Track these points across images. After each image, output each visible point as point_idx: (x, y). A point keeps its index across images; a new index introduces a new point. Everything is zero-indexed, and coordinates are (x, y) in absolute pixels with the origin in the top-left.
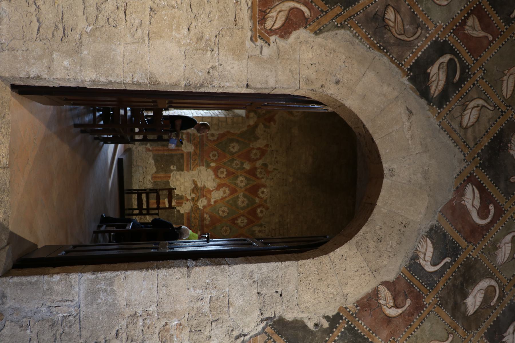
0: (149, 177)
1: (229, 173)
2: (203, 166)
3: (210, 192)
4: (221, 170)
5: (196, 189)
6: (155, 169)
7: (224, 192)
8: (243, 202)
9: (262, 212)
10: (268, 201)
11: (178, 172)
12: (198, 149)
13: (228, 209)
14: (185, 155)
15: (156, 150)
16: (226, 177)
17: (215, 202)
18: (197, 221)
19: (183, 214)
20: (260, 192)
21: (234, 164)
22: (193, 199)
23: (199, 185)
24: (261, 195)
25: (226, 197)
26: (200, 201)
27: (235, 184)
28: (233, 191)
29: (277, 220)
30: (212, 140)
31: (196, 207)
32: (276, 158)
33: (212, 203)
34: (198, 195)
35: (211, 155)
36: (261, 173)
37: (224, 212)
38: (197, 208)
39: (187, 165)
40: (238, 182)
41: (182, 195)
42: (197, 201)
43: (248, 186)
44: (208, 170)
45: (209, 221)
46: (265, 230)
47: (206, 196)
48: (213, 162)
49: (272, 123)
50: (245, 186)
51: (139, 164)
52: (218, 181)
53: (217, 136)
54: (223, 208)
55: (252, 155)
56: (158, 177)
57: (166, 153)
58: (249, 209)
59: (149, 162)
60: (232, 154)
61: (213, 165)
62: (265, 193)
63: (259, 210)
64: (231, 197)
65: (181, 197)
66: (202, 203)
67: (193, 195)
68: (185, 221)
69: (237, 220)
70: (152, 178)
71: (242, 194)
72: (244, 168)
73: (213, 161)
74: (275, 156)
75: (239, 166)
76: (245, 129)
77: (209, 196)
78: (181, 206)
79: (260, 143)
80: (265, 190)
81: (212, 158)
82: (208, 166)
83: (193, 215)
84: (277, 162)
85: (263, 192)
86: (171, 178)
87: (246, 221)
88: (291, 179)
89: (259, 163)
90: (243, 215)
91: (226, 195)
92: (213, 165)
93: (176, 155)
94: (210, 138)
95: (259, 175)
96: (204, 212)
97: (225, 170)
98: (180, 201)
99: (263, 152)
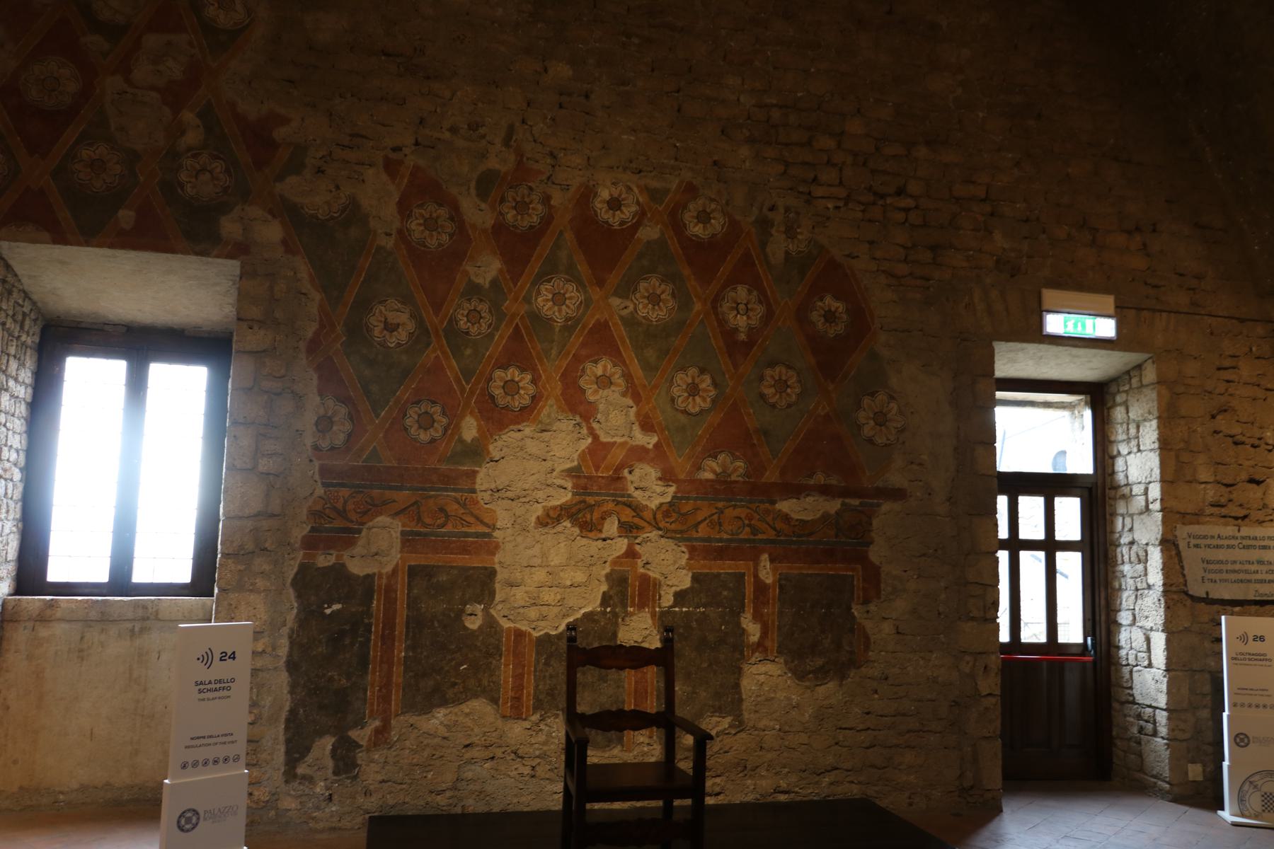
0: (517, 731)
1: (517, 355)
2: (475, 473)
3: (598, 450)
4: (498, 392)
5: (581, 516)
6: (479, 705)
7: (604, 382)
8: (654, 300)
9: (704, 217)
10: (655, 184)
11: (498, 598)
12: (389, 494)
13: (683, 369)
14: (415, 560)
15: (386, 699)
16: (534, 370)
17: (647, 426)
18: (730, 513)
19: (695, 578)
20: (614, 219)
21: (474, 330)
22: (627, 529)
23: (565, 497)
24: (628, 212)
25: (628, 376)
26: (637, 494)
27: (569, 328)
28: (601, 340)
29: (745, 151)
30: (348, 427)
31: (667, 514)
32: (454, 130)
33: (651, 441)
34: (611, 506)
35: (424, 437)
36: (522, 207)
37: (693, 390)
38: (669, 509)
39: (464, 550)
40: (558, 315)
41: (608, 576)
42: (637, 509)
43: (583, 268)
44: (496, 454)
45: (736, 458)
46: (787, 210)
47: (619, 469)
48: (458, 427)
49: (280, 133)
50: (581, 285)
51: (449, 777)
52: (549, 409)
53: (330, 403)
54: (675, 391)
55: (432, 243)
56: (519, 688)
57: (400, 652)
58: (686, 272)
59: (442, 731)
60: (422, 336)
61: (470, 429)
62: (617, 196)
63: (697, 230)
64: (629, 354)
65: (618, 581)
66: (649, 488)
67: (611, 527)
68: (726, 567)
69: (736, 330)
70: (519, 717)
71: (615, 302)
72: (494, 283)
73: (453, 427)
74: (447, 135)
75: (484, 308)
76: (303, 269)
77: (618, 456)
78: (657, 585)
79: (379, 198)
80: (605, 194)
81: (436, 432)
82: (476, 452)
83: (703, 531)
84: (474, 127)
85: (615, 204)
86: (524, 627)
87: (742, 292)
88: (561, 70)
89: (478, 214)
90: (716, 301)
91: (617, 374)
92: (470, 429)
93: (413, 603)
94: (340, 439)
95: (534, 218)
96: (692, 481)
97: (498, 373)
98: (633, 587)
99: (422, 190)
